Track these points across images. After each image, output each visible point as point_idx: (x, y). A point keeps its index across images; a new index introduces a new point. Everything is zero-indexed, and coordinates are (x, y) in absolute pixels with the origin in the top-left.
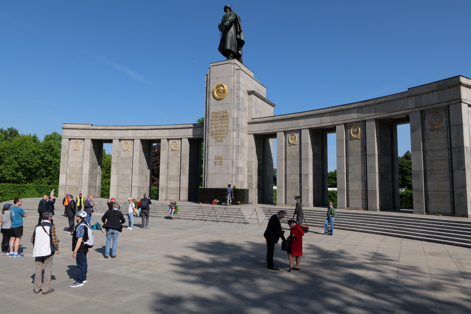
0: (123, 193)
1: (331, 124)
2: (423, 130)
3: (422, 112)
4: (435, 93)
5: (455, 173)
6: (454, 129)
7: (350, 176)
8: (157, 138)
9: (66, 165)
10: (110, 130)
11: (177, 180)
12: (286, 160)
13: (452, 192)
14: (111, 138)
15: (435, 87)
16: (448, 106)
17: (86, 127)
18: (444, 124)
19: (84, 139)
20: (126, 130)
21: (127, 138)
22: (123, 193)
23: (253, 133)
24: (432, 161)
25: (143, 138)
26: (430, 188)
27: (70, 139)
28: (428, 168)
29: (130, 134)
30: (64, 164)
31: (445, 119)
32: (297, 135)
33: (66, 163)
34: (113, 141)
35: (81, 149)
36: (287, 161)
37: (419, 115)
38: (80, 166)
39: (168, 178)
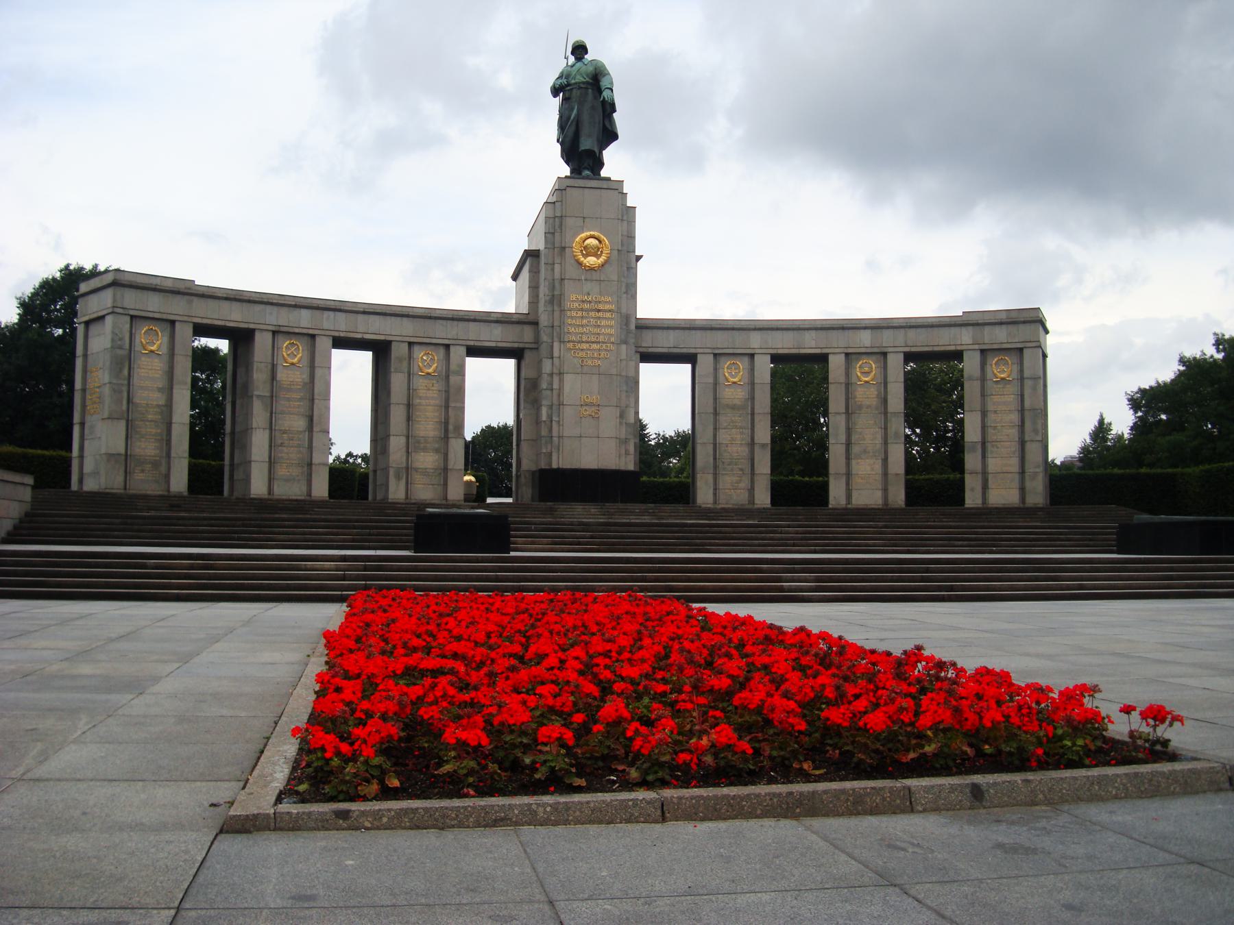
0: (287, 480)
1: (818, 351)
3: (982, 351)
4: (1004, 327)
5: (1028, 446)
6: (1028, 383)
7: (855, 449)
8: (382, 338)
9: (125, 394)
10: (249, 301)
11: (437, 451)
12: (716, 413)
13: (1022, 472)
14: (252, 326)
15: (1003, 317)
16: (1021, 350)
17: (181, 287)
18: (1015, 375)
19: (173, 323)
20: (296, 306)
21: (297, 330)
22: (287, 480)
23: (641, 350)
24: (995, 428)
25: (342, 335)
27: (132, 317)
28: (990, 437)
29: (304, 320)
30: (121, 392)
31: (1016, 368)
32: (743, 364)
33: (125, 389)
34: (258, 336)
35: (164, 350)
37: (978, 354)
38: (162, 402)
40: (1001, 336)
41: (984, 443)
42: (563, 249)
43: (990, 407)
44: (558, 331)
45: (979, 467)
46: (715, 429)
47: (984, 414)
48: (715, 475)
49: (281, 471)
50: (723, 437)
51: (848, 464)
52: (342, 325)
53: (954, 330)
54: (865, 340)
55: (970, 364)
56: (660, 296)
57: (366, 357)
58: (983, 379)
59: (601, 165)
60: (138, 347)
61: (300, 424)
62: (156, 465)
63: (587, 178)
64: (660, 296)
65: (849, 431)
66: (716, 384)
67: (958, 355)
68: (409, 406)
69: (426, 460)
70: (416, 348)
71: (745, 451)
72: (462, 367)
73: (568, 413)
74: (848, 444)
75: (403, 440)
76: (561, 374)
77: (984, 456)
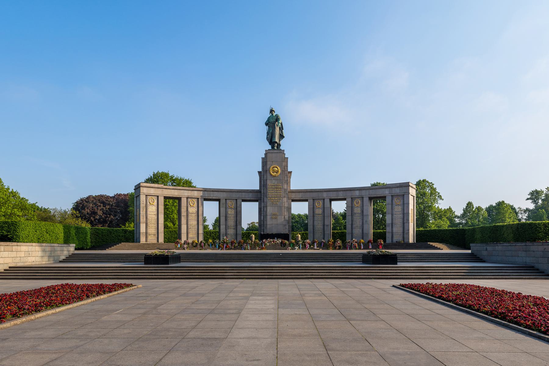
2: (392, 204)
5: (405, 224)
6: (405, 205)
7: (354, 226)
12: (314, 216)
18: (402, 203)
19: (158, 196)
26: (394, 231)
28: (394, 222)
29: (196, 194)
31: (402, 200)
32: (321, 202)
34: (182, 199)
36: (315, 218)
37: (390, 197)
39: (226, 228)
40: (397, 191)
41: (392, 224)
42: (266, 171)
43: (394, 213)
44: (265, 195)
45: (391, 231)
46: (313, 221)
47: (392, 215)
48: (313, 234)
49: (190, 236)
50: (316, 223)
51: (352, 230)
52: (207, 195)
53: (383, 190)
54: (357, 193)
55: (389, 199)
56: (296, 183)
57: (218, 202)
58: (392, 204)
59: (280, 145)
60: (148, 203)
61: (196, 223)
62: (154, 235)
63: (275, 150)
64: (296, 183)
65: (352, 221)
66: (313, 208)
67: (384, 198)
68: (226, 217)
69: (231, 231)
70: (228, 201)
71: (322, 227)
72: (241, 205)
73: (268, 217)
74: (352, 225)
75: (224, 226)
76: (266, 207)
77: (392, 228)
